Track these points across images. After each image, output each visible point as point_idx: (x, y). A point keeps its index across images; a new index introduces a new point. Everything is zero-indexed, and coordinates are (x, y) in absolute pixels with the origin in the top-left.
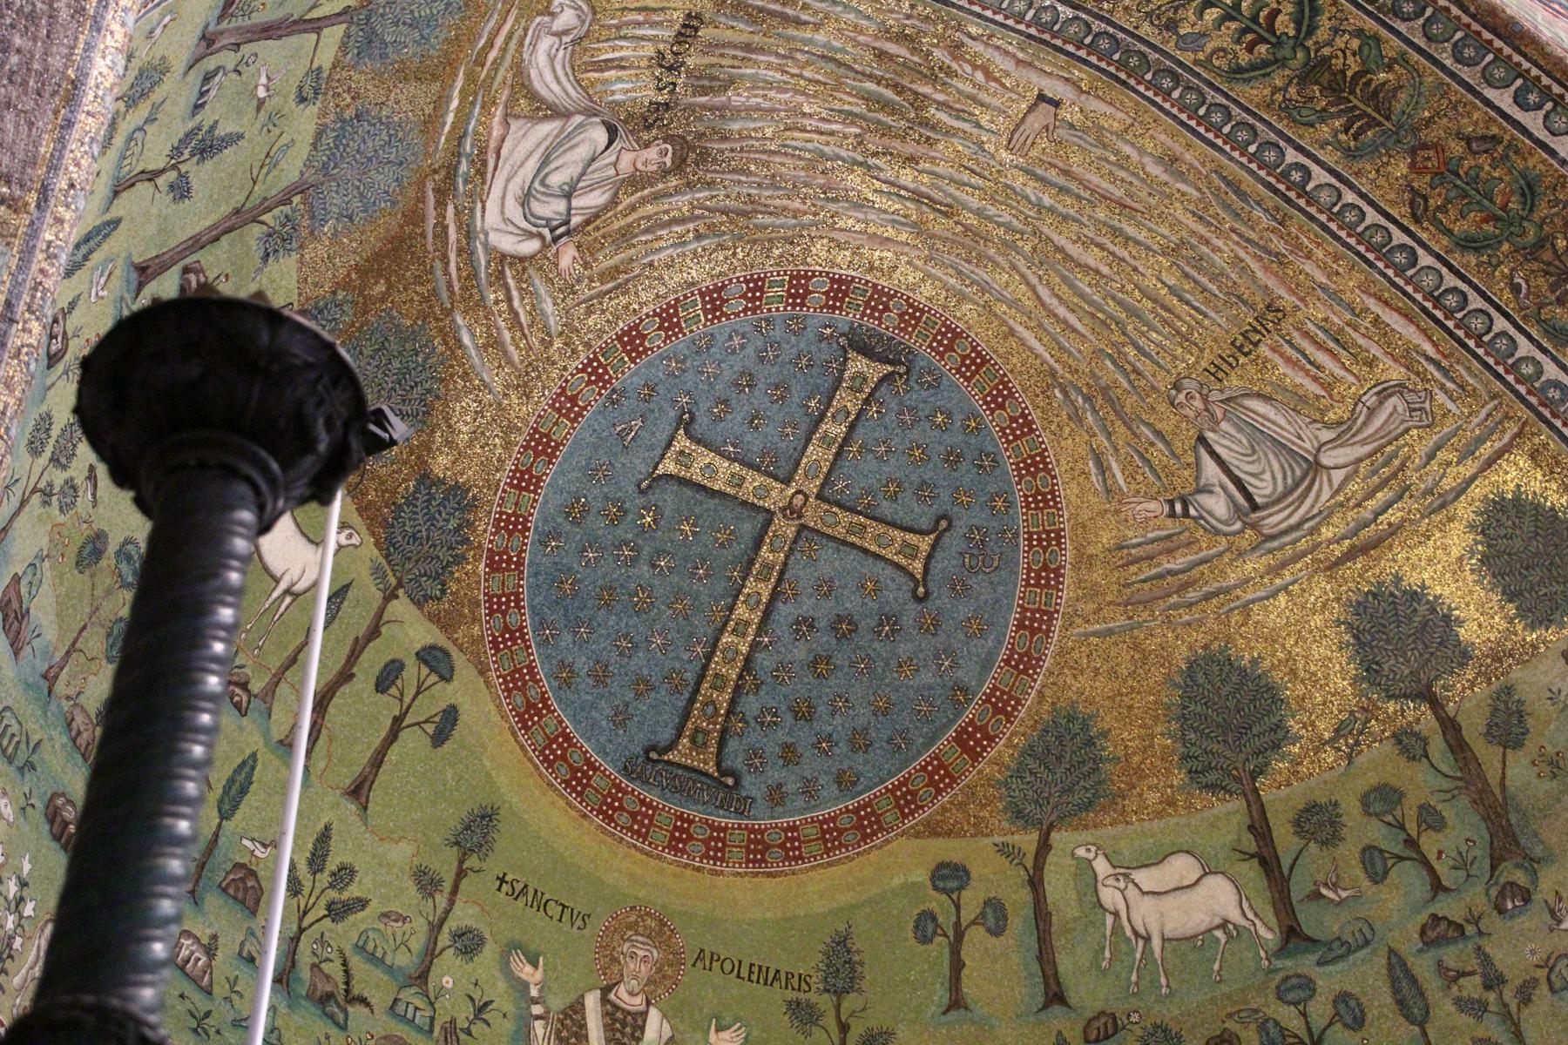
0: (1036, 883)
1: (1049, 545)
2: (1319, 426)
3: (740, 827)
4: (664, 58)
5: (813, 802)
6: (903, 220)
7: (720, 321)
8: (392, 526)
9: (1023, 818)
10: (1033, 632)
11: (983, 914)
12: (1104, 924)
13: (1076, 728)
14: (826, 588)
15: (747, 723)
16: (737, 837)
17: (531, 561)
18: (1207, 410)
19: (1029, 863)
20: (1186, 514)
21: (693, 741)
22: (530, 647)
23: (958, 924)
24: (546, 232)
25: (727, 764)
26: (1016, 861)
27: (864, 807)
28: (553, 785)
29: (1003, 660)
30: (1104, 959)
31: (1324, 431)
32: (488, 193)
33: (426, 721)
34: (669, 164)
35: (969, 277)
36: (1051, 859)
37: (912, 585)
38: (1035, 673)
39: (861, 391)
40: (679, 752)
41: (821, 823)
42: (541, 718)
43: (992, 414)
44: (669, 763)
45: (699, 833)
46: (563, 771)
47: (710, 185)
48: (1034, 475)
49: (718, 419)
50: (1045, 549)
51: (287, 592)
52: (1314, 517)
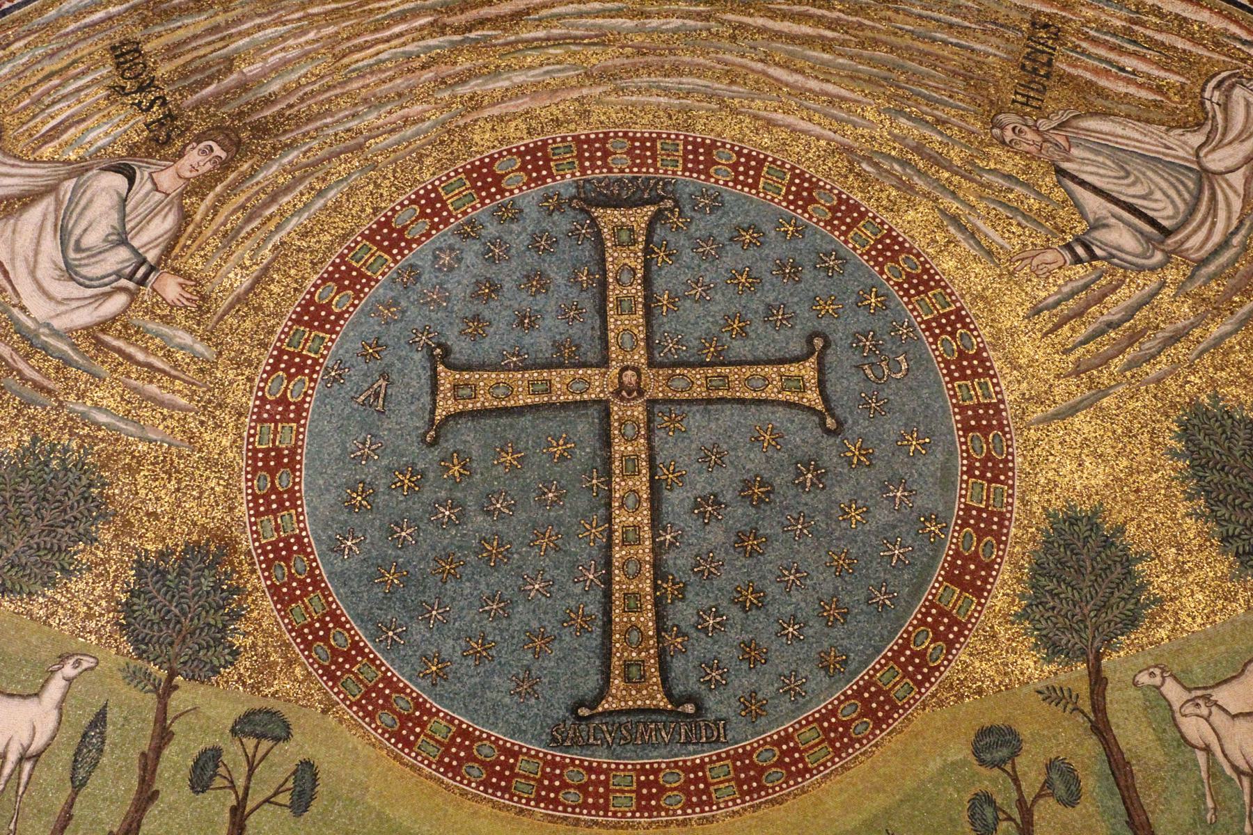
0: (1101, 728)
1: (955, 330)
2: (1180, 131)
3: (720, 758)
4: (123, 88)
5: (801, 700)
6: (558, 67)
7: (411, 250)
8: (129, 625)
9: (1061, 652)
10: (985, 431)
11: (1048, 783)
12: (1197, 766)
13: (1083, 527)
14: (712, 457)
15: (684, 635)
16: (719, 772)
17: (330, 574)
18: (1045, 141)
19: (1087, 708)
20: (1093, 257)
21: (627, 679)
22: (376, 658)
23: (1021, 802)
24: (123, 282)
25: (678, 689)
26: (1070, 706)
27: (866, 688)
28: (467, 793)
29: (963, 473)
30: (1207, 810)
31: (1189, 135)
32: (18, 295)
33: (275, 794)
34: (223, 155)
35: (680, 89)
36: (1111, 695)
37: (816, 419)
38: (1008, 478)
39: (635, 242)
40: (614, 697)
41: (819, 721)
42: (423, 725)
43: (805, 211)
44: (610, 713)
45: (674, 781)
46: (475, 772)
47: (291, 146)
48: (894, 259)
49: (476, 337)
50: (952, 334)
51: (21, 760)
52: (1237, 229)
